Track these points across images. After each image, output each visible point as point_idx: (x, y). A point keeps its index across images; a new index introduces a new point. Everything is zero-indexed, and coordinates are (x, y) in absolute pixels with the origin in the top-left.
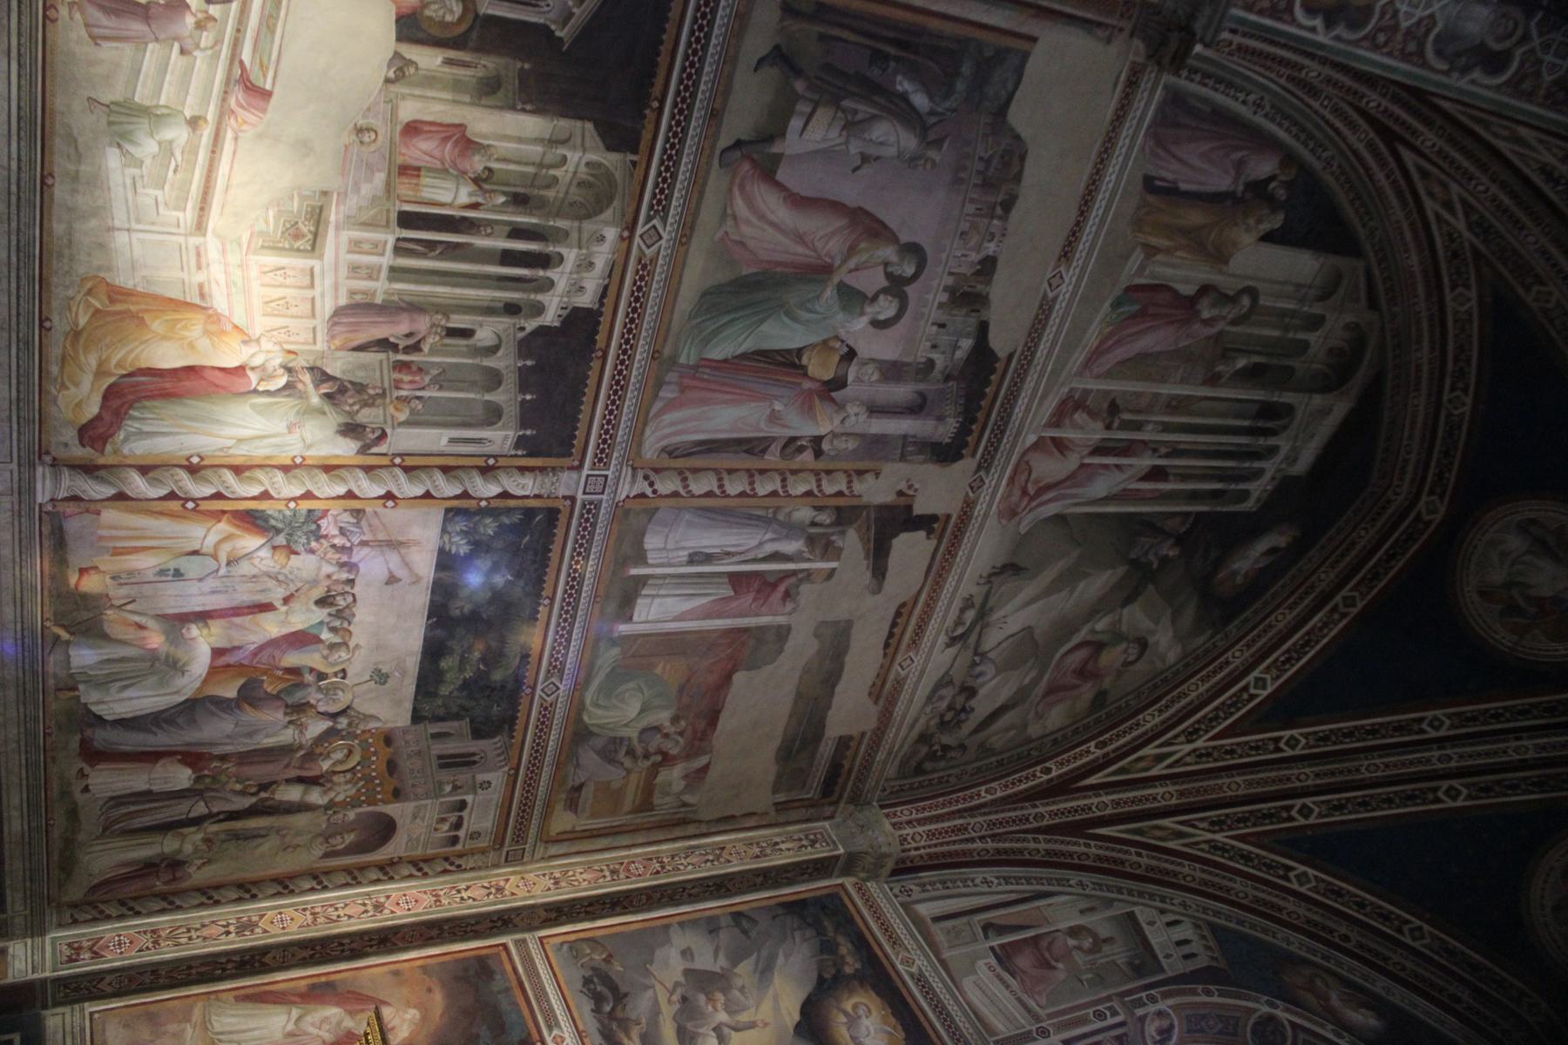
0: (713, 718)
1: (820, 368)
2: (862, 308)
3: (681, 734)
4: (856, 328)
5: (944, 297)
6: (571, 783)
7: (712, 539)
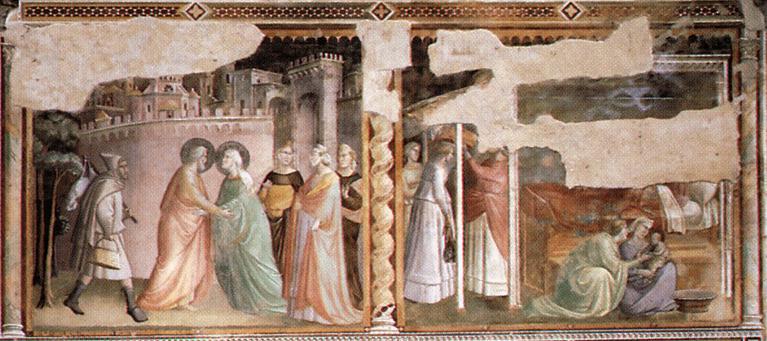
0: (618, 194)
1: (284, 197)
2: (235, 179)
3: (629, 222)
4: (250, 179)
5: (219, 112)
6: (676, 312)
7: (433, 243)
